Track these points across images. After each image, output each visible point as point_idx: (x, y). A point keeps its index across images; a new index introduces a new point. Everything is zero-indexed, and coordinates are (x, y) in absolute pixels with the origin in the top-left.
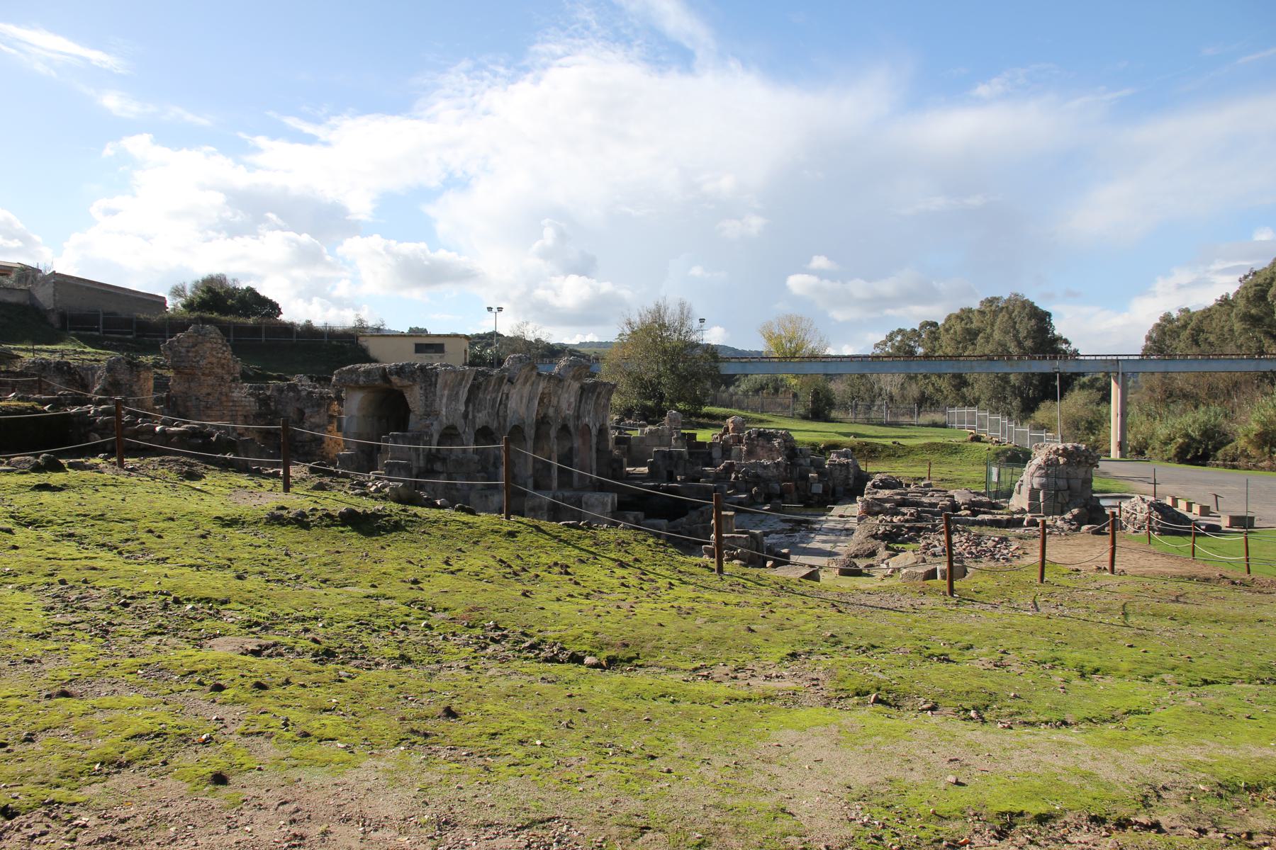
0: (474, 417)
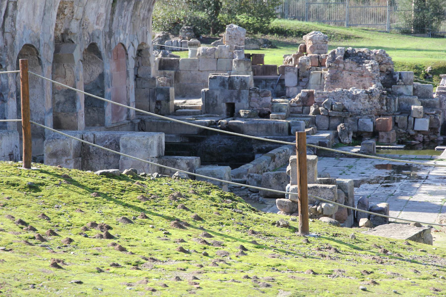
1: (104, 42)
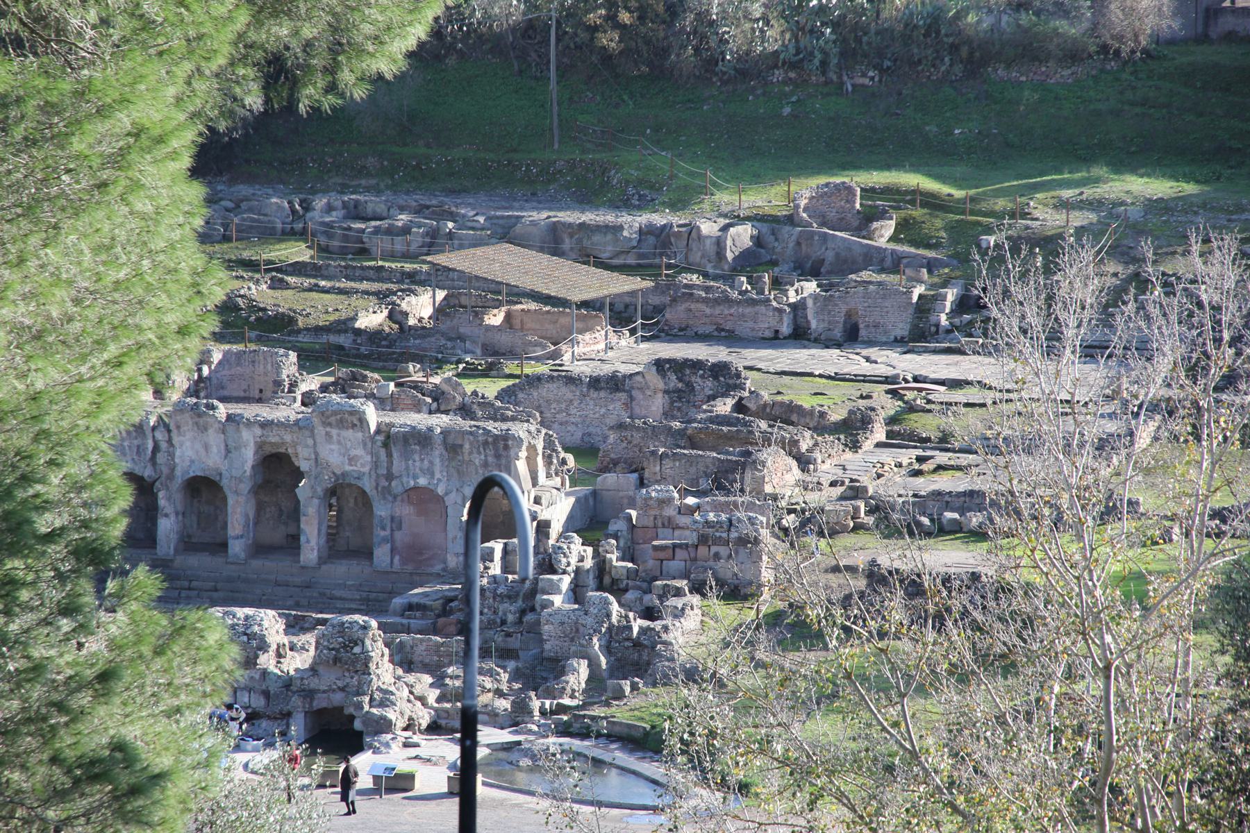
1: (374, 484)
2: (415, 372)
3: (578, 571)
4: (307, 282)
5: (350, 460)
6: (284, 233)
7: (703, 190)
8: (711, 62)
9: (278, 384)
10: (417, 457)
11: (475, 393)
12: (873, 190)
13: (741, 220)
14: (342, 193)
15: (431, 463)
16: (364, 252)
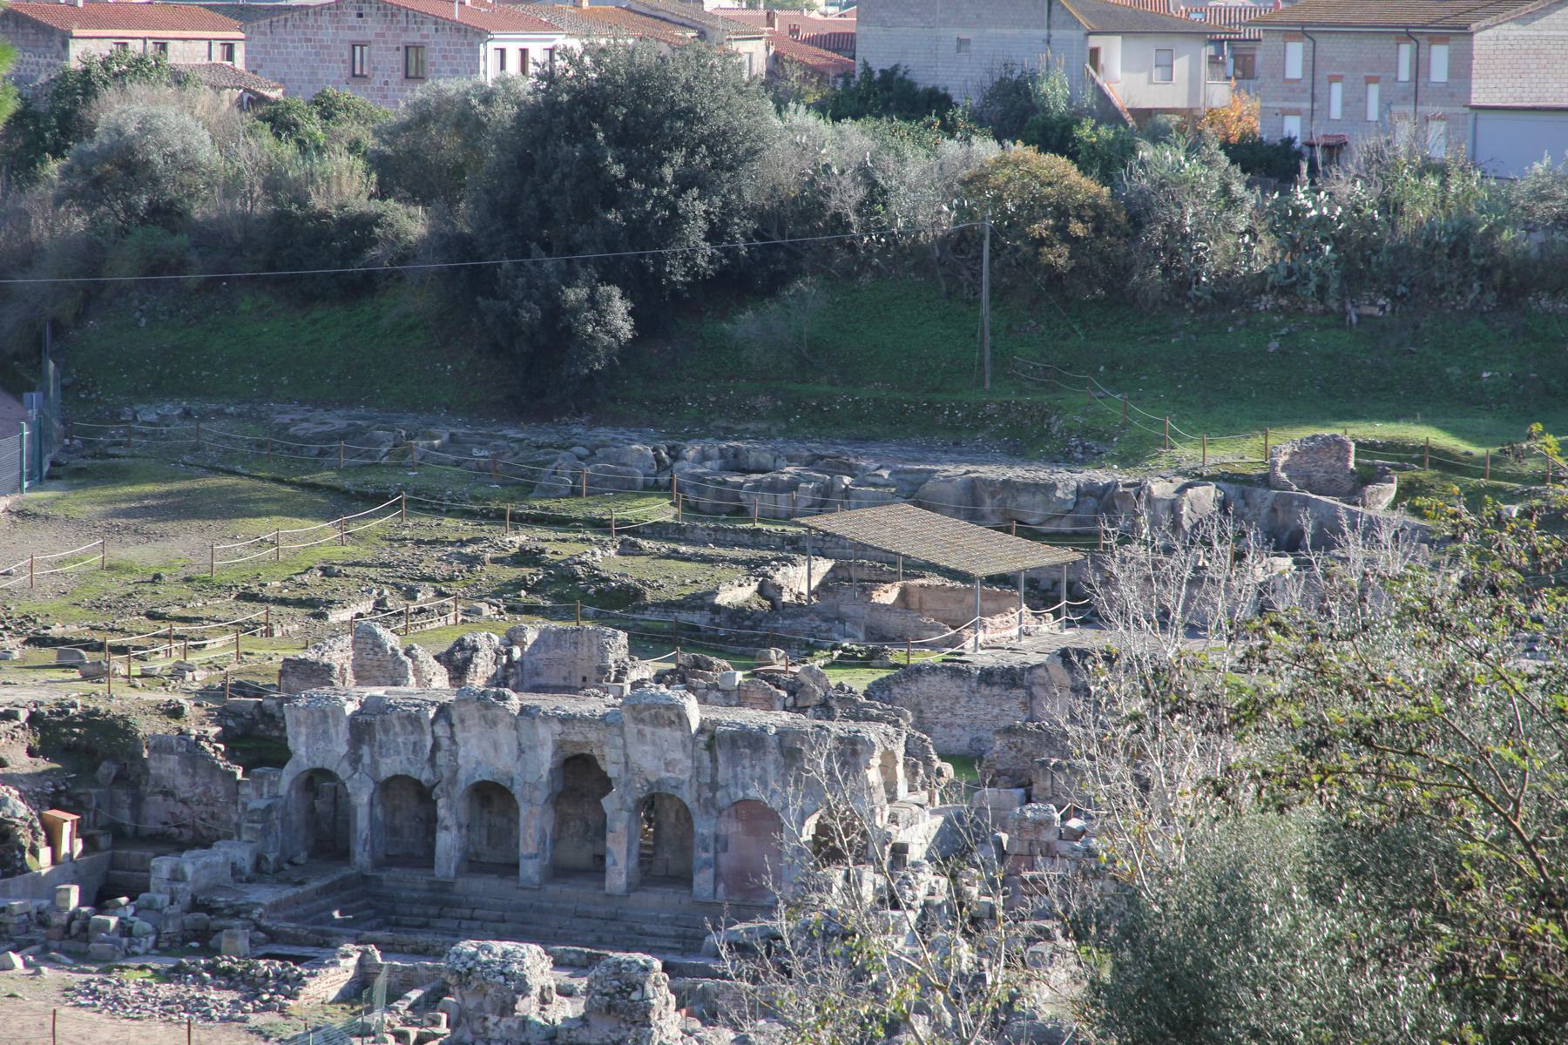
0: (375, 764)
2: (777, 659)
3: (927, 905)
4: (666, 547)
5: (667, 764)
6: (646, 487)
7: (1160, 442)
8: (1182, 285)
9: (603, 670)
10: (746, 762)
11: (840, 687)
12: (1373, 445)
13: (1202, 479)
14: (724, 439)
15: (764, 769)
16: (741, 512)
